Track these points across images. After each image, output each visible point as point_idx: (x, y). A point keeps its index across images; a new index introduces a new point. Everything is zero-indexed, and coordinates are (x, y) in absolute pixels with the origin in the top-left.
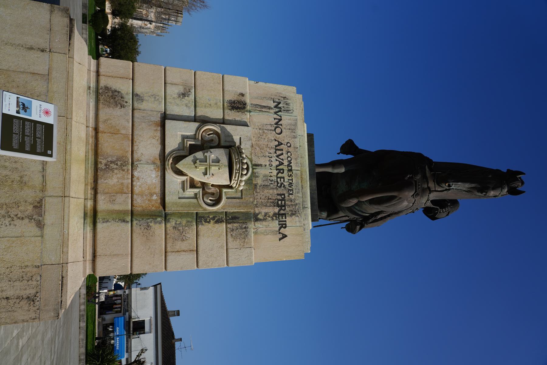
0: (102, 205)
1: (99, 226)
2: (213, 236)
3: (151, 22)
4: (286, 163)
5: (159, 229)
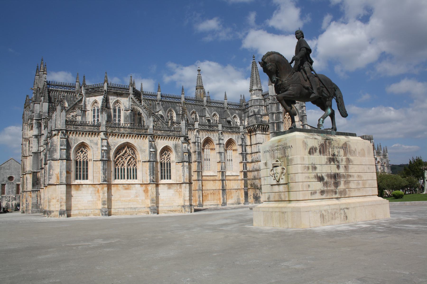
0: (287, 199)
1: (291, 200)
2: (292, 169)
4: (276, 148)
5: (291, 185)
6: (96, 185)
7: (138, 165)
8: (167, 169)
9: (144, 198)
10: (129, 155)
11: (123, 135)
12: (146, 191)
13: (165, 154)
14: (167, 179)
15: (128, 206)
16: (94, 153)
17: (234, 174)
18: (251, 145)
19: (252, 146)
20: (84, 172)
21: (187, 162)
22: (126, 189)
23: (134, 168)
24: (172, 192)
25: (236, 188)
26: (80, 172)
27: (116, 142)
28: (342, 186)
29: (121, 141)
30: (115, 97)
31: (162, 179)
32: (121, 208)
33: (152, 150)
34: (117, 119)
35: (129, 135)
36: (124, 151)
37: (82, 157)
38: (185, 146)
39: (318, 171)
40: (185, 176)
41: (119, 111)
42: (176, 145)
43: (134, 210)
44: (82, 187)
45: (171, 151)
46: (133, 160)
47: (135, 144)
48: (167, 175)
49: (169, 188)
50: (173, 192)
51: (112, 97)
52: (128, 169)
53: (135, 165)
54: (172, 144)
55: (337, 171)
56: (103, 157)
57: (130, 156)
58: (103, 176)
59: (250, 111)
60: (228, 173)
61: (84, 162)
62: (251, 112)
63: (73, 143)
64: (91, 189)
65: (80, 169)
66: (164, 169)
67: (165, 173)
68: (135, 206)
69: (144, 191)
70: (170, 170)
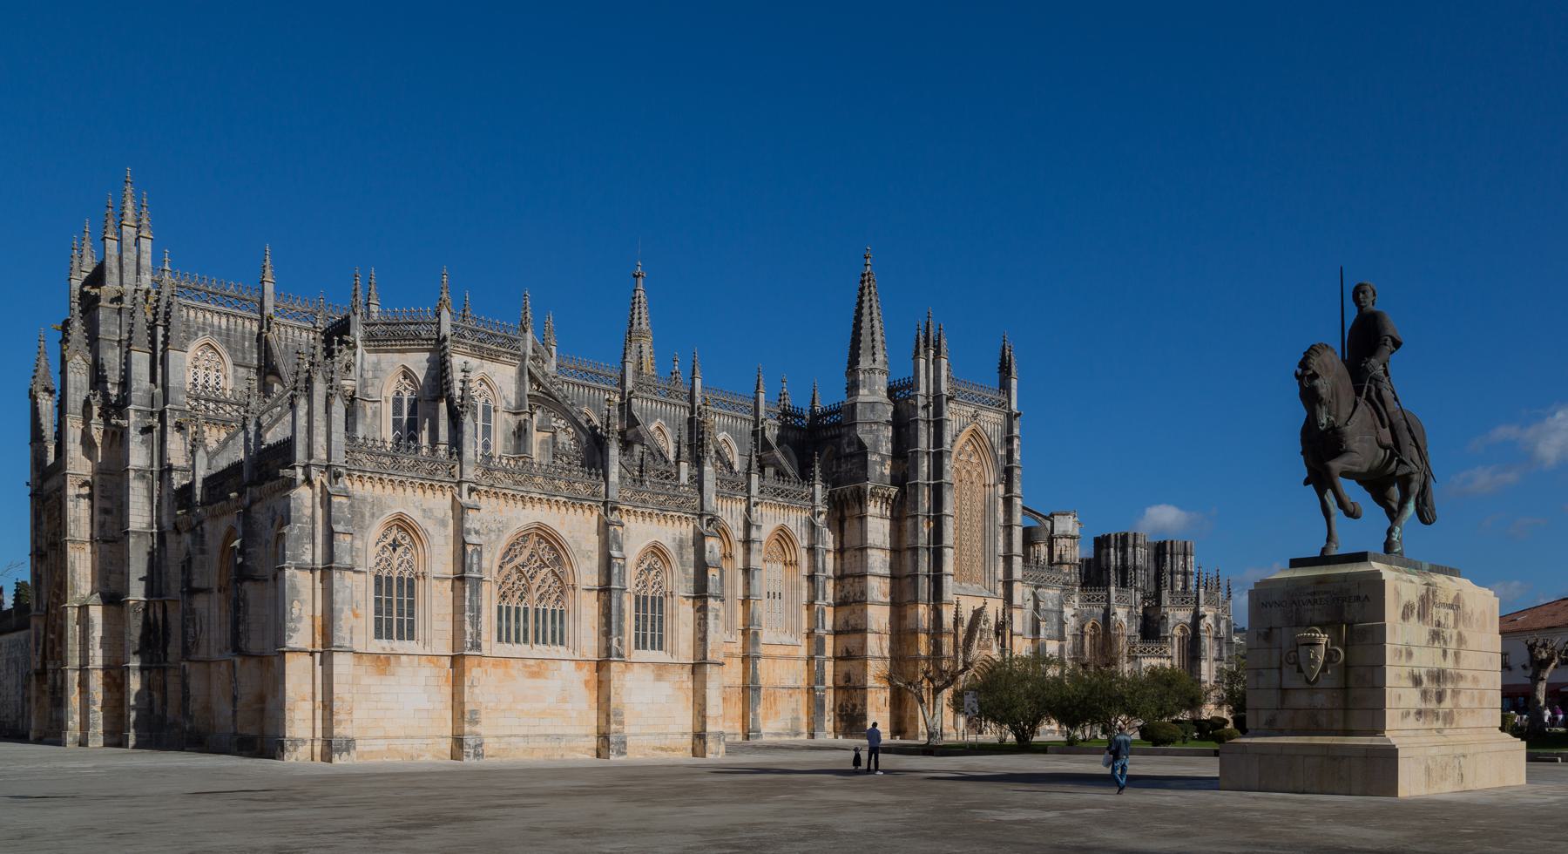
3: (1197, 617)
13: (649, 569)
14: (653, 648)
17: (786, 639)
19: (847, 555)
20: (400, 613)
21: (716, 597)
25: (790, 683)
26: (390, 613)
28: (1448, 703)
31: (637, 647)
33: (615, 553)
35: (549, 498)
36: (526, 553)
37: (396, 563)
39: (1414, 662)
40: (710, 641)
44: (399, 664)
47: (563, 532)
49: (659, 678)
52: (537, 610)
54: (670, 537)
55: (1443, 665)
57: (545, 570)
59: (845, 440)
60: (766, 636)
61: (400, 579)
62: (850, 444)
64: (426, 671)
65: (389, 602)
66: (645, 617)
70: (661, 619)
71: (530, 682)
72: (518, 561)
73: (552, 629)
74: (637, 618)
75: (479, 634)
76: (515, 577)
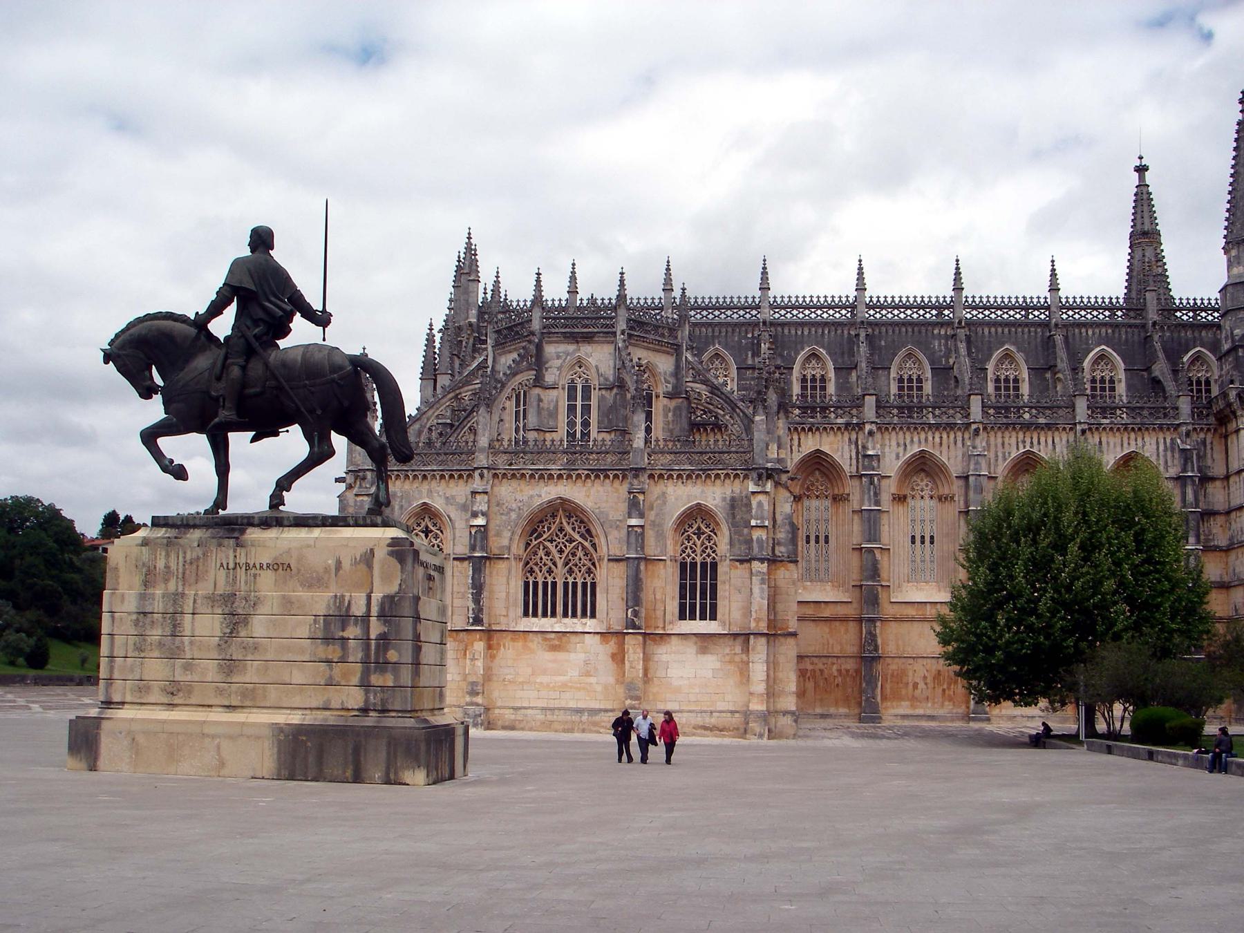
6: (461, 634)
7: (598, 573)
8: (703, 587)
9: (611, 680)
10: (571, 541)
11: (545, 477)
12: (619, 658)
14: (703, 618)
15: (557, 704)
16: (457, 535)
18: (1227, 477)
19: (1232, 480)
21: (762, 560)
22: (554, 648)
23: (589, 580)
24: (710, 665)
27: (525, 498)
29: (549, 492)
30: (571, 348)
31: (682, 617)
32: (536, 708)
33: (633, 522)
34: (579, 420)
38: (760, 504)
41: (587, 390)
42: (733, 499)
43: (575, 718)
45: (718, 524)
46: (586, 554)
48: (703, 607)
49: (703, 650)
50: (718, 665)
51: (562, 348)
52: (566, 584)
53: (589, 572)
54: (718, 501)
56: (473, 548)
58: (472, 606)
63: (397, 507)
66: (693, 587)
67: (693, 597)
68: (581, 705)
69: (613, 656)
70: (714, 588)
71: (549, 656)
72: (545, 536)
73: (581, 601)
74: (682, 587)
75: (481, 610)
76: (541, 553)
